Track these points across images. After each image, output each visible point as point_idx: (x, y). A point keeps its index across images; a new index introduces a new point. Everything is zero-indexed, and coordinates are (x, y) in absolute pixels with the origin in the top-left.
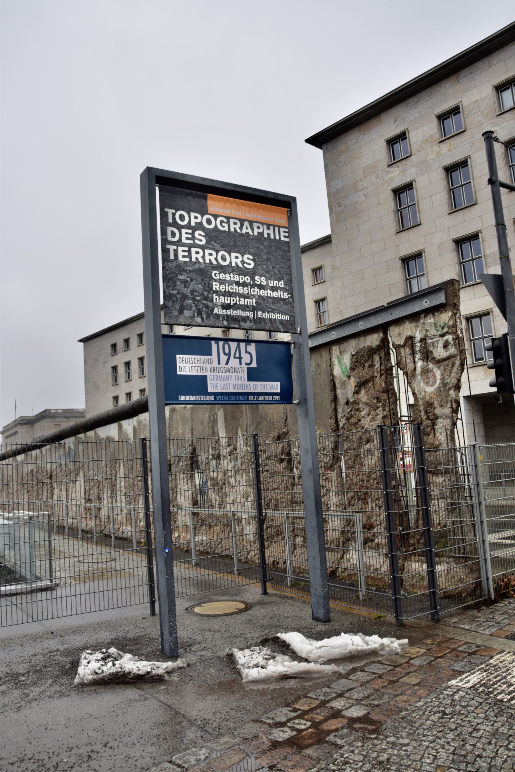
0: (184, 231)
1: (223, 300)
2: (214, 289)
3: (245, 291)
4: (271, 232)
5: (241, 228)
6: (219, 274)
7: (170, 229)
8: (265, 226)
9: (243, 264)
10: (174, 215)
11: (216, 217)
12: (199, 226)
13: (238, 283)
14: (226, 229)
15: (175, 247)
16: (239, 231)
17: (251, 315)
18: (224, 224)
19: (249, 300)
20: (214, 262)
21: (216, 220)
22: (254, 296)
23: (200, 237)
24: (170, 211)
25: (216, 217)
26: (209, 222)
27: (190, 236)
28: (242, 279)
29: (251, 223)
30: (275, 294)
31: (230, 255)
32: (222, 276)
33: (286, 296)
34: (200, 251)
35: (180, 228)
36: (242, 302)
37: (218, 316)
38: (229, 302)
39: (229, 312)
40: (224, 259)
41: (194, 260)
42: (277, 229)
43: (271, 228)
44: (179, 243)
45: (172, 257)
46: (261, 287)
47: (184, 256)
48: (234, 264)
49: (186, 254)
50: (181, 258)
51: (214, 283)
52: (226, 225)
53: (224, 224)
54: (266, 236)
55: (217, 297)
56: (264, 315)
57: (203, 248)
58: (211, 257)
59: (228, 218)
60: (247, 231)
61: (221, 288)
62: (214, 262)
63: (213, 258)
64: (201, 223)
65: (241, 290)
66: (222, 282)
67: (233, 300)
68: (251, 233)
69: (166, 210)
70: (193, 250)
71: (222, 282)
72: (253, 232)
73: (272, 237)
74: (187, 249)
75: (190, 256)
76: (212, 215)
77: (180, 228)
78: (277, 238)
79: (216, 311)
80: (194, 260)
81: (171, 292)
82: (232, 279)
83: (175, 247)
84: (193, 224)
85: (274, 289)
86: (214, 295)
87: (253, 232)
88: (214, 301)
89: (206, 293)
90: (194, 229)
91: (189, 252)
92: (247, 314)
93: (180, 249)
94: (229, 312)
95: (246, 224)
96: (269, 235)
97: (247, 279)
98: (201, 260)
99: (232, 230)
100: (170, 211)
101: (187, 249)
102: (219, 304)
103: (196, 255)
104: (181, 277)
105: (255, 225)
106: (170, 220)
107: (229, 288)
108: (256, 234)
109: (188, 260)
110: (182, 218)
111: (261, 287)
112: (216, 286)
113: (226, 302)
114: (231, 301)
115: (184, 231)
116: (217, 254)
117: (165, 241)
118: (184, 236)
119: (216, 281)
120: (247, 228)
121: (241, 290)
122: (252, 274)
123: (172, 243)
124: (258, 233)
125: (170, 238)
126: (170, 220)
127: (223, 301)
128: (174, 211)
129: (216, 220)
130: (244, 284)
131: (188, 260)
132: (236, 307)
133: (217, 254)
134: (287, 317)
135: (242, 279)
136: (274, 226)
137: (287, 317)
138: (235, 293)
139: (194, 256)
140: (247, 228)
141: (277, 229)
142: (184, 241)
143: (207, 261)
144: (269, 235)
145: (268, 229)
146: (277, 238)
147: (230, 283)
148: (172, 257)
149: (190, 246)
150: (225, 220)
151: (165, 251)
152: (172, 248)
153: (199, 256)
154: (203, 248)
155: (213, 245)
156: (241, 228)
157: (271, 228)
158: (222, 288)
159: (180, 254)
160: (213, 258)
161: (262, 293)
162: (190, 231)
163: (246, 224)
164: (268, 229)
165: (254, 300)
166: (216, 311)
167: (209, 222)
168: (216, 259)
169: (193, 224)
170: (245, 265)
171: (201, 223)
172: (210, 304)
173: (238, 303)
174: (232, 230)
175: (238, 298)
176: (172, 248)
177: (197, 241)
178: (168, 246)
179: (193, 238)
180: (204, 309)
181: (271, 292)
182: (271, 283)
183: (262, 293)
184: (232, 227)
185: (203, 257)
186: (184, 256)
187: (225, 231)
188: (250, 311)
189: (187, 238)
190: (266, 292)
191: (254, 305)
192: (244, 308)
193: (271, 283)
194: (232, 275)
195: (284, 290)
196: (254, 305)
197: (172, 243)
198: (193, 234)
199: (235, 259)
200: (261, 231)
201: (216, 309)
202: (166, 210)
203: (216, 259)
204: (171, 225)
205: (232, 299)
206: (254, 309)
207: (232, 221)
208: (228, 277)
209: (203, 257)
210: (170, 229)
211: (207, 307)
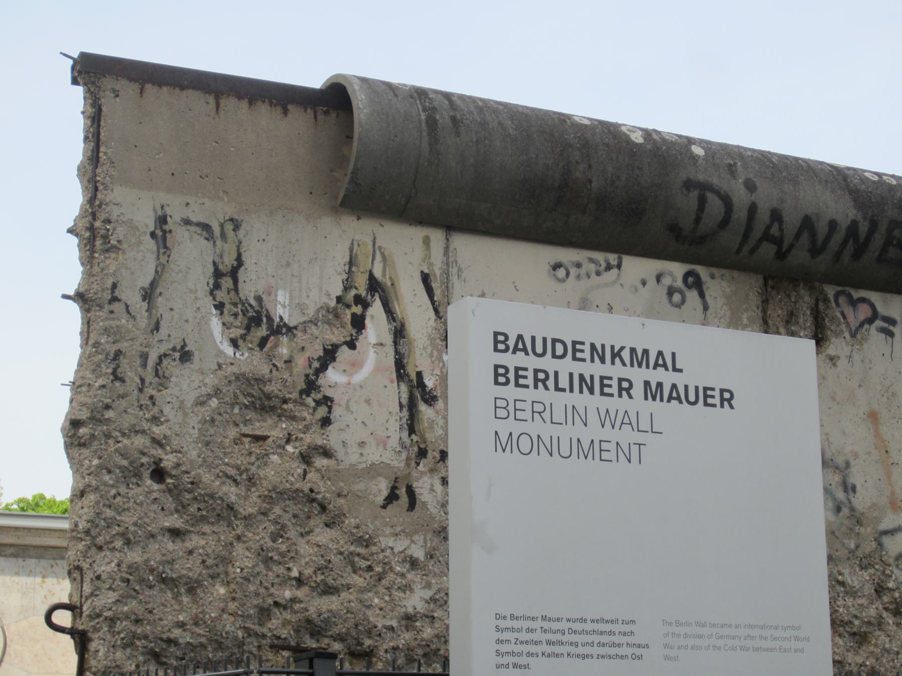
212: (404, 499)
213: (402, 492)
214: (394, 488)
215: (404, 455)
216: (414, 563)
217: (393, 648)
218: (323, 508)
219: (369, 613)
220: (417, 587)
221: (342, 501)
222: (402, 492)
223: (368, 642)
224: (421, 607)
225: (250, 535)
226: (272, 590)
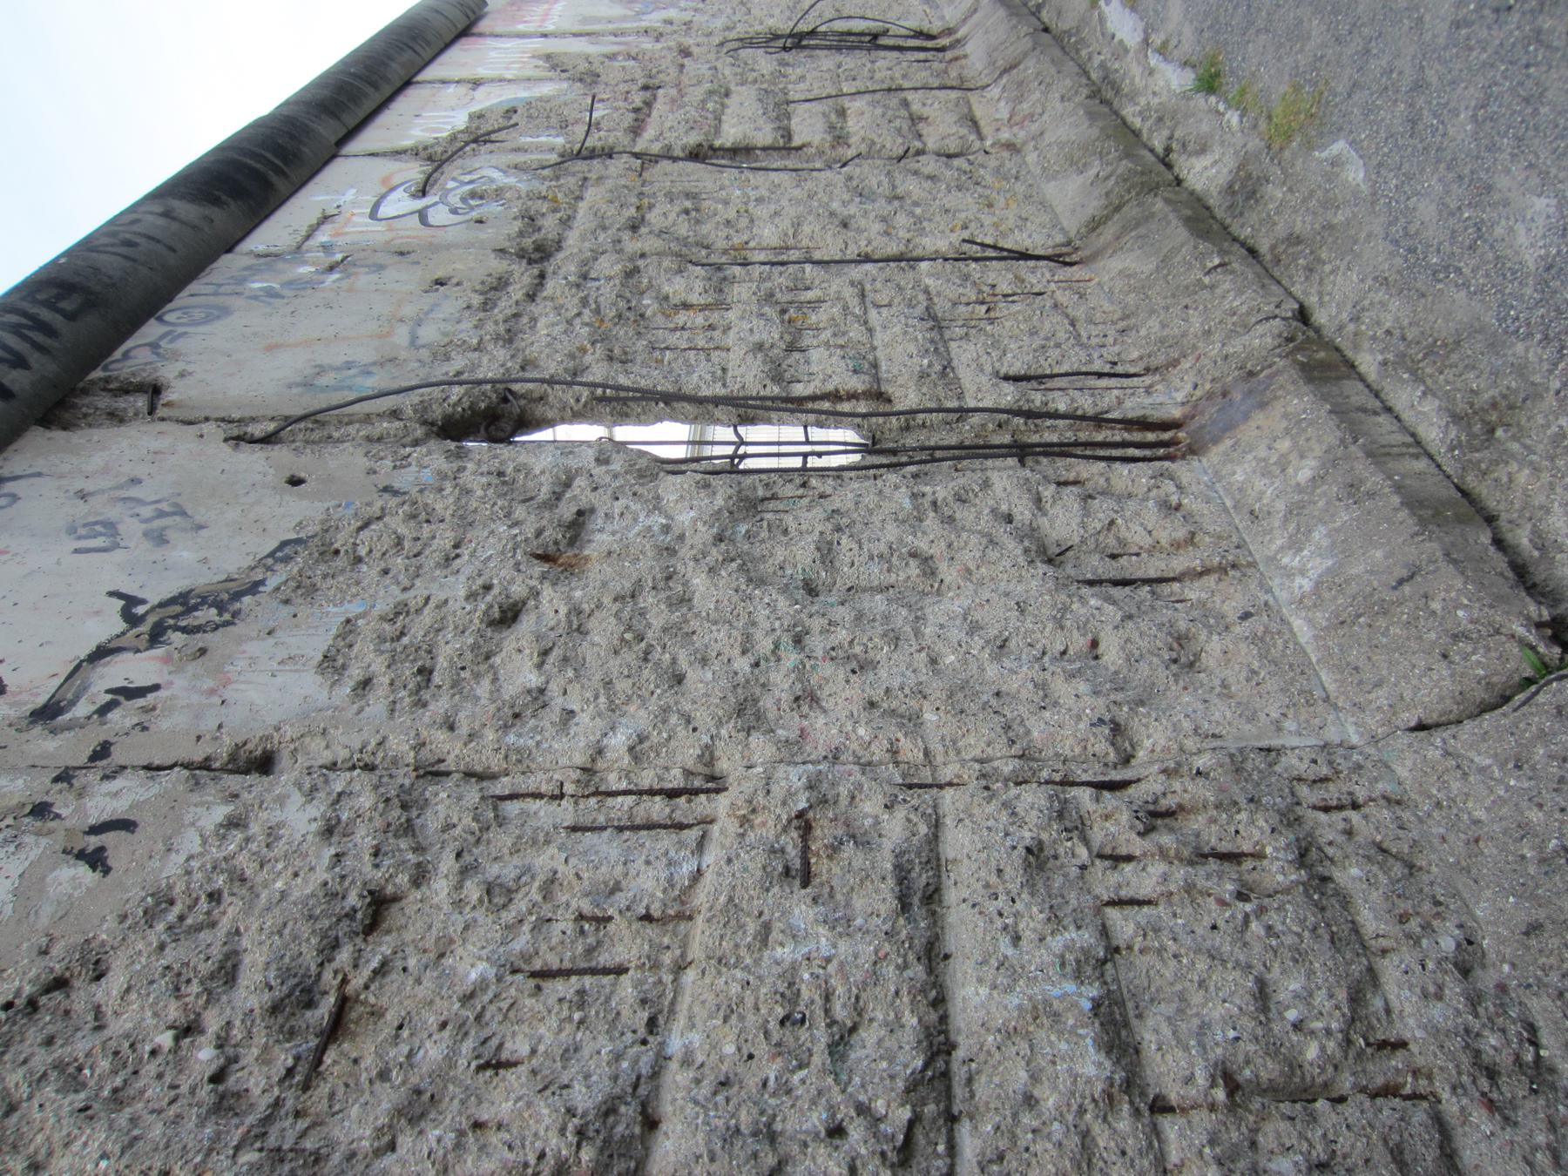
212: (108, 839)
213: (94, 842)
214: (81, 855)
215: (28, 839)
216: (234, 823)
217: (376, 855)
218: (60, 984)
219: (296, 894)
220: (276, 816)
221: (57, 950)
222: (94, 842)
223: (353, 899)
224: (318, 809)
225: (39, 1138)
226: (184, 1089)
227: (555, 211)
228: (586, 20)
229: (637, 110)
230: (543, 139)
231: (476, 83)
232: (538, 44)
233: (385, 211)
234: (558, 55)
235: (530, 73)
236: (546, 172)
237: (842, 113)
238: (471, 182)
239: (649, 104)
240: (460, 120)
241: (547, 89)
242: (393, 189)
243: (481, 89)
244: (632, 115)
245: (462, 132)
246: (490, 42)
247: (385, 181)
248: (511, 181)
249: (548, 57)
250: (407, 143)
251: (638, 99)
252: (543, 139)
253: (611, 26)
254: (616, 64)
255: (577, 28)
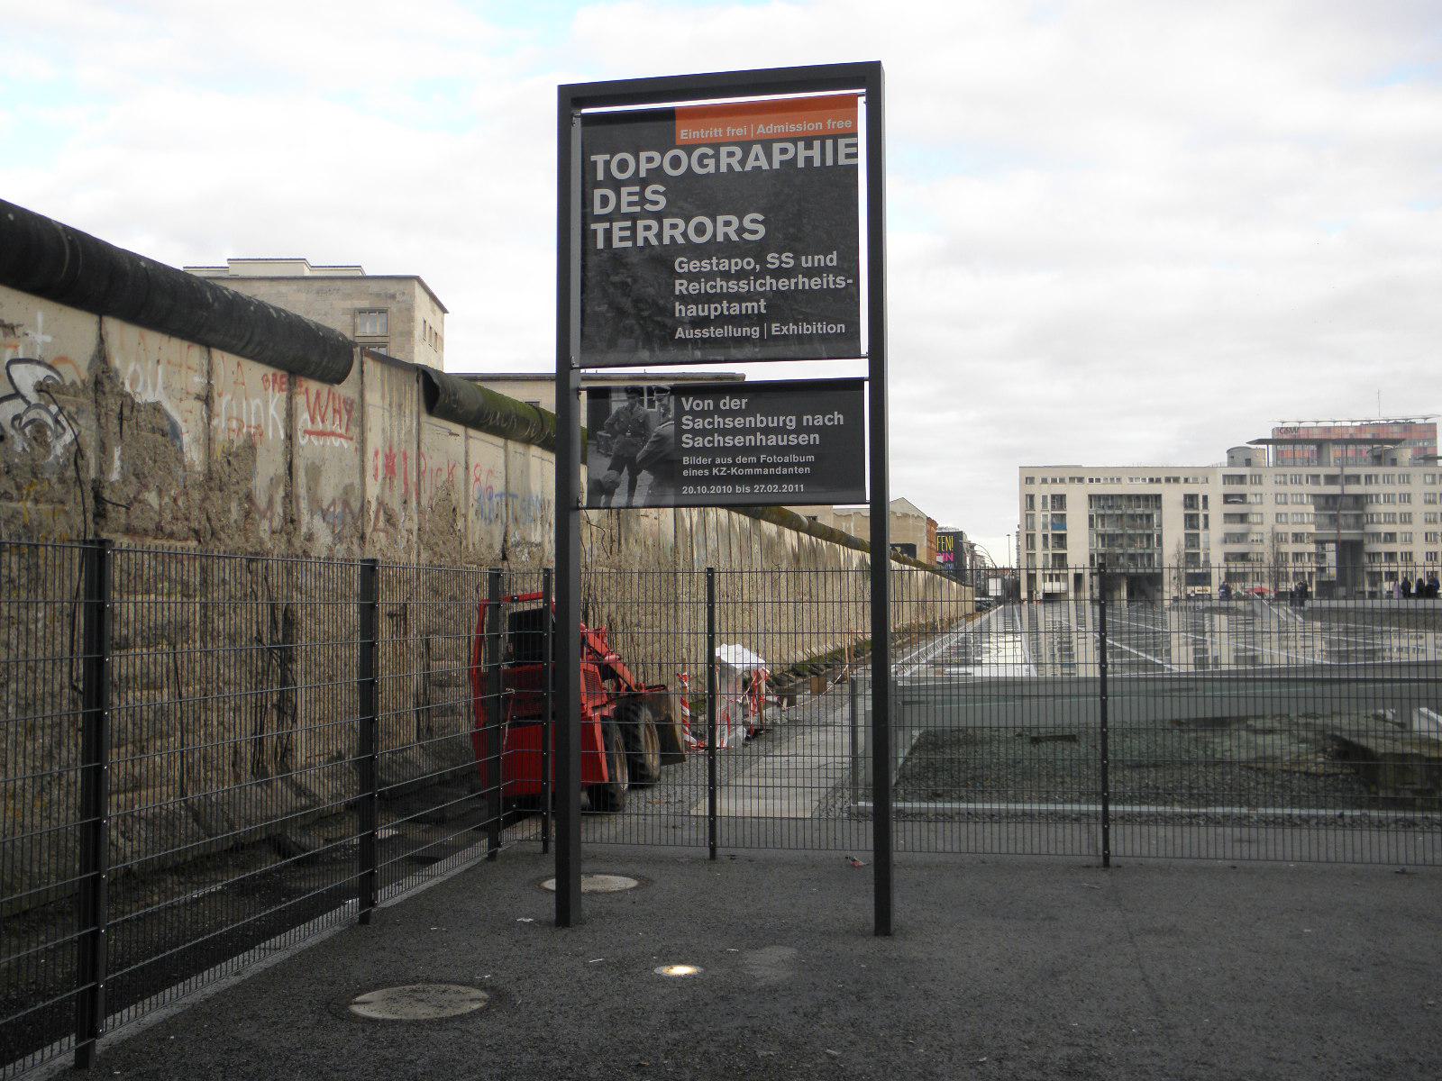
0: (624, 191)
1: (693, 311)
2: (677, 293)
3: (743, 286)
4: (815, 153)
5: (743, 162)
6: (688, 263)
7: (598, 193)
8: (801, 145)
9: (739, 235)
10: (607, 163)
11: (689, 148)
12: (657, 175)
13: (726, 275)
14: (711, 169)
15: (607, 225)
16: (738, 168)
17: (755, 332)
18: (706, 161)
19: (749, 305)
20: (680, 240)
21: (689, 157)
22: (762, 294)
23: (657, 196)
24: (600, 159)
25: (689, 148)
26: (676, 162)
27: (636, 198)
28: (735, 265)
29: (767, 145)
30: (815, 283)
31: (714, 222)
32: (694, 266)
33: (841, 282)
34: (654, 224)
35: (617, 185)
36: (736, 309)
37: (683, 343)
38: (706, 313)
39: (706, 333)
40: (700, 230)
41: (640, 243)
42: (829, 143)
43: (817, 144)
44: (616, 215)
45: (600, 245)
46: (779, 273)
47: (622, 239)
48: (720, 238)
49: (628, 233)
50: (616, 244)
51: (677, 282)
52: (711, 162)
53: (706, 161)
54: (801, 164)
55: (683, 308)
56: (785, 329)
57: (659, 216)
58: (675, 230)
59: (716, 146)
60: (757, 164)
61: (691, 288)
62: (680, 240)
63: (677, 234)
64: (661, 167)
65: (733, 286)
66: (692, 277)
67: (716, 309)
68: (765, 166)
69: (593, 158)
70: (641, 224)
71: (692, 277)
72: (770, 163)
73: (817, 163)
74: (628, 224)
75: (634, 237)
76: (682, 147)
77: (617, 185)
78: (829, 162)
79: (680, 333)
80: (640, 243)
81: (597, 309)
82: (715, 269)
83: (607, 225)
84: (643, 174)
85: (810, 273)
86: (677, 304)
87: (770, 163)
88: (677, 315)
89: (661, 302)
90: (644, 183)
91: (633, 229)
92: (746, 331)
93: (617, 225)
94: (706, 333)
95: (757, 149)
96: (809, 160)
97: (749, 263)
98: (654, 242)
99: (723, 169)
100: (600, 159)
101: (628, 224)
102: (686, 320)
103: (647, 233)
104: (616, 279)
105: (776, 147)
106: (600, 176)
107: (706, 287)
108: (776, 165)
109: (629, 244)
110: (623, 166)
111: (779, 273)
112: (680, 286)
113: (701, 314)
114: (712, 310)
115: (624, 191)
116: (687, 224)
117: (587, 217)
118: (625, 199)
119: (681, 276)
120: (757, 159)
121: (733, 286)
122: (759, 250)
123: (601, 219)
124: (782, 163)
125: (598, 210)
126: (600, 176)
127: (694, 314)
128: (607, 157)
129: (689, 157)
130: (741, 275)
131: (629, 244)
132: (722, 320)
133: (687, 224)
134: (841, 328)
135: (735, 265)
136: (823, 139)
137: (841, 328)
138: (722, 293)
139: (641, 234)
140: (757, 159)
141: (829, 143)
142: (625, 209)
143: (666, 241)
144: (809, 160)
145: (809, 146)
146: (829, 162)
147: (710, 276)
148: (600, 245)
149: (634, 218)
150: (710, 152)
151: (587, 236)
152: (600, 228)
153: (651, 235)
154: (659, 216)
155: (682, 208)
156: (743, 162)
157: (817, 144)
158: (694, 288)
159: (616, 234)
160: (677, 234)
161: (783, 284)
162: (637, 189)
163: (757, 149)
164: (809, 146)
165: (762, 303)
166: (680, 333)
167: (676, 162)
168: (685, 234)
169: (643, 174)
170: (747, 236)
171: (661, 167)
172: (669, 322)
173: (726, 313)
174: (723, 169)
175: (725, 304)
176: (600, 228)
177: (648, 207)
178: (593, 226)
179: (643, 201)
180: (657, 332)
181: (806, 280)
182: (806, 262)
183: (783, 284)
184: (724, 161)
185: (659, 236)
186: (622, 239)
187: (708, 174)
188: (751, 326)
189: (630, 204)
190: (793, 281)
191: (763, 311)
192: (738, 320)
193: (806, 262)
194: (714, 260)
195: (836, 271)
196: (763, 311)
197: (601, 219)
198: (641, 194)
199: (724, 227)
200: (789, 156)
201: (680, 329)
202: (593, 158)
203: (685, 234)
204: (599, 185)
205: (713, 306)
206: (759, 320)
207: (724, 151)
208: (705, 266)
209: (659, 236)
210: (598, 193)
211: (664, 326)
227: (19, 488)
228: (315, 472)
229: (159, 528)
230: (117, 463)
231: (207, 400)
232: (275, 432)
233: (19, 372)
234: (254, 455)
235: (221, 437)
236: (70, 473)
237: (152, 685)
238: (57, 422)
239: (171, 535)
240: (146, 396)
241: (194, 455)
242: (50, 367)
243: (198, 406)
244: (151, 526)
245: (133, 401)
246: (277, 400)
247: (63, 359)
248: (59, 450)
249: (250, 447)
250: (116, 362)
251: (179, 527)
252: (117, 463)
253: (302, 491)
254: (234, 506)
255: (300, 464)
